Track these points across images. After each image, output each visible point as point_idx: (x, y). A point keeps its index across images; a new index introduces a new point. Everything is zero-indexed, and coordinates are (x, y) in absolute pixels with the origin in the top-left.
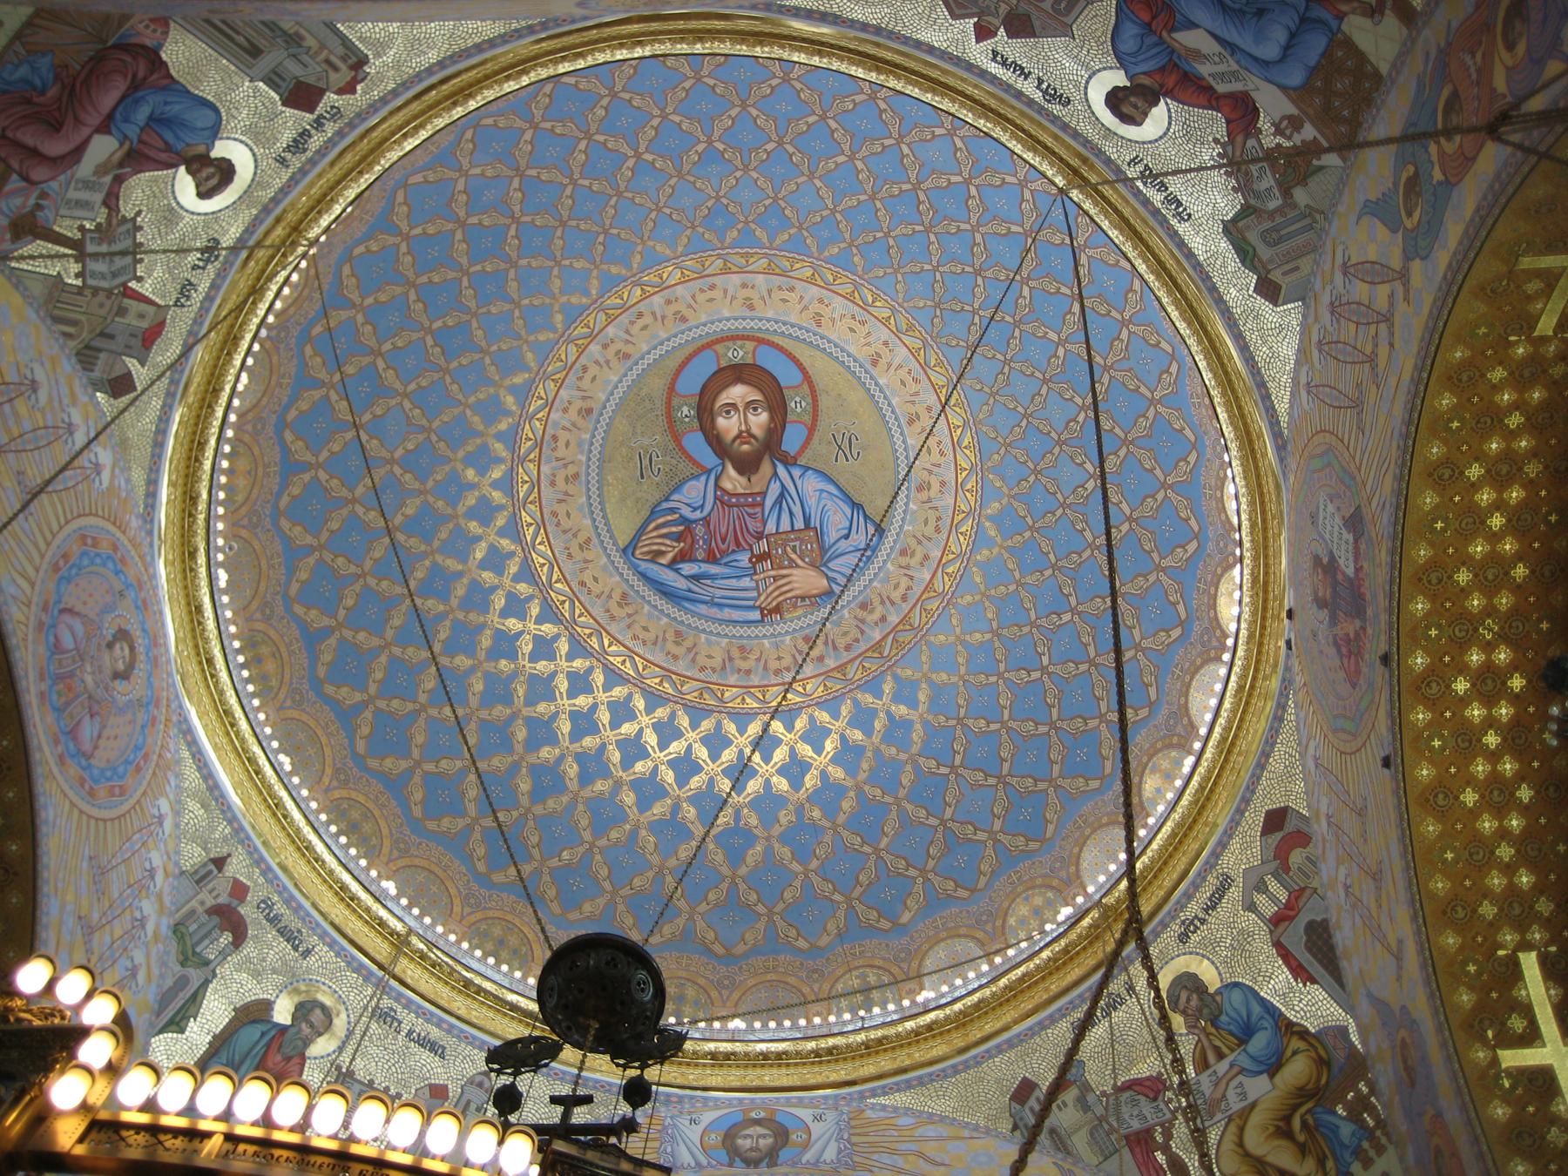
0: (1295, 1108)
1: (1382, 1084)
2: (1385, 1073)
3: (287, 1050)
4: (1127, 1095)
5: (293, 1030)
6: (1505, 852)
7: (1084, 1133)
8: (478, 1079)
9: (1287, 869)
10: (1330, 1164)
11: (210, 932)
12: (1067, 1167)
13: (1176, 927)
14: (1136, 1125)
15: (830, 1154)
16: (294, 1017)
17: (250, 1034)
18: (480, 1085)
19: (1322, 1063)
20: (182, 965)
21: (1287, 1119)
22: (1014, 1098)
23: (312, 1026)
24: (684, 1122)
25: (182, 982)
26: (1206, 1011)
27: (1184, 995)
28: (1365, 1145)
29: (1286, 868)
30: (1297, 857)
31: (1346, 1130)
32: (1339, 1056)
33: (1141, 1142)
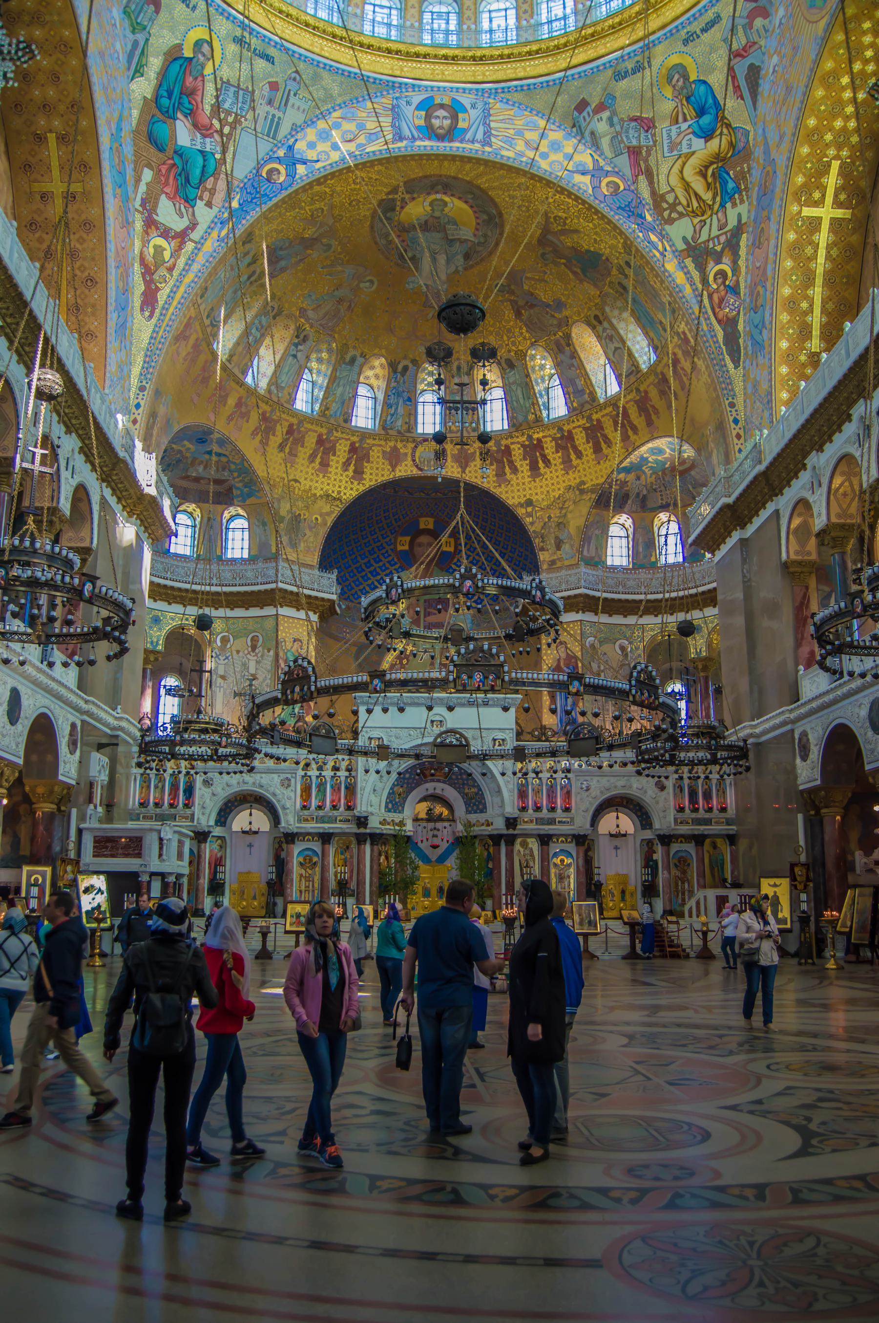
0: (712, 163)
1: (754, 172)
2: (756, 176)
3: (194, 73)
4: (633, 124)
5: (195, 60)
6: (850, 109)
7: (608, 138)
8: (294, 75)
9: (751, 28)
10: (718, 199)
11: (142, 8)
12: (596, 157)
13: (683, 33)
14: (635, 143)
15: (480, 136)
16: (194, 52)
17: (175, 67)
18: (295, 79)
19: (731, 145)
20: (133, 32)
21: (707, 168)
22: (576, 109)
23: (204, 55)
24: (403, 103)
25: (136, 43)
26: (685, 91)
27: (676, 77)
28: (736, 196)
29: (750, 25)
30: (758, 22)
31: (731, 185)
32: (741, 145)
33: (634, 153)
